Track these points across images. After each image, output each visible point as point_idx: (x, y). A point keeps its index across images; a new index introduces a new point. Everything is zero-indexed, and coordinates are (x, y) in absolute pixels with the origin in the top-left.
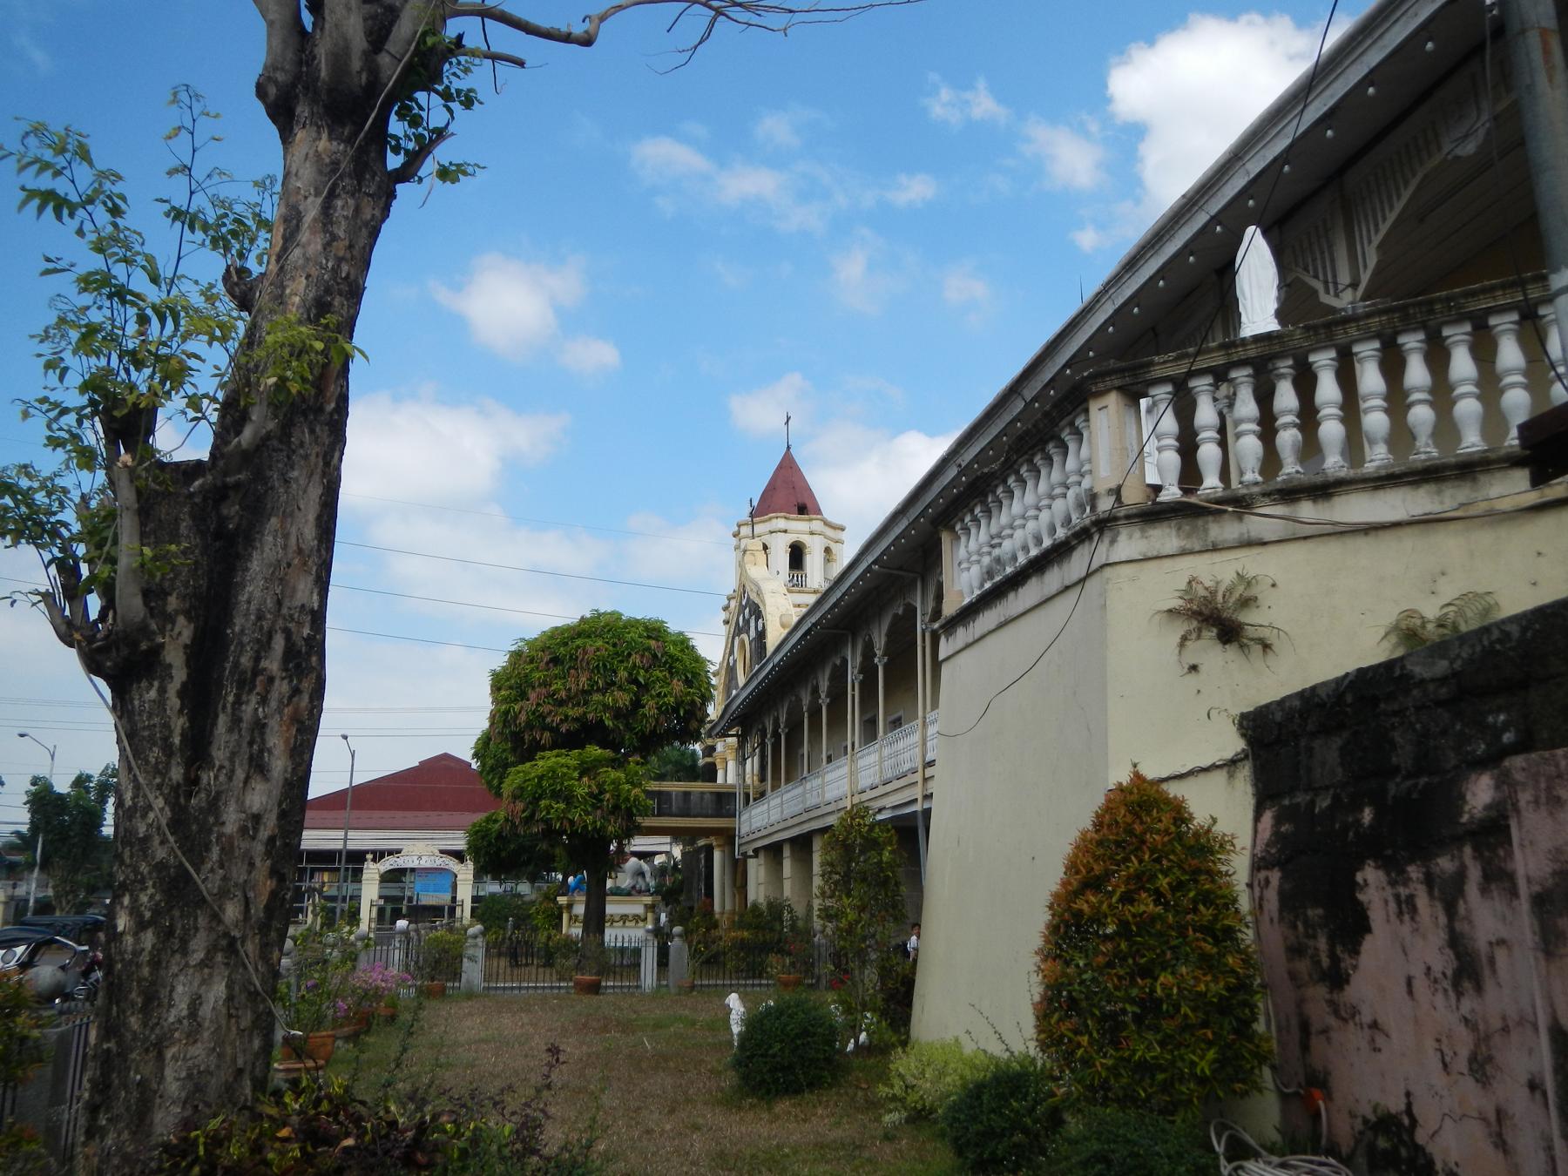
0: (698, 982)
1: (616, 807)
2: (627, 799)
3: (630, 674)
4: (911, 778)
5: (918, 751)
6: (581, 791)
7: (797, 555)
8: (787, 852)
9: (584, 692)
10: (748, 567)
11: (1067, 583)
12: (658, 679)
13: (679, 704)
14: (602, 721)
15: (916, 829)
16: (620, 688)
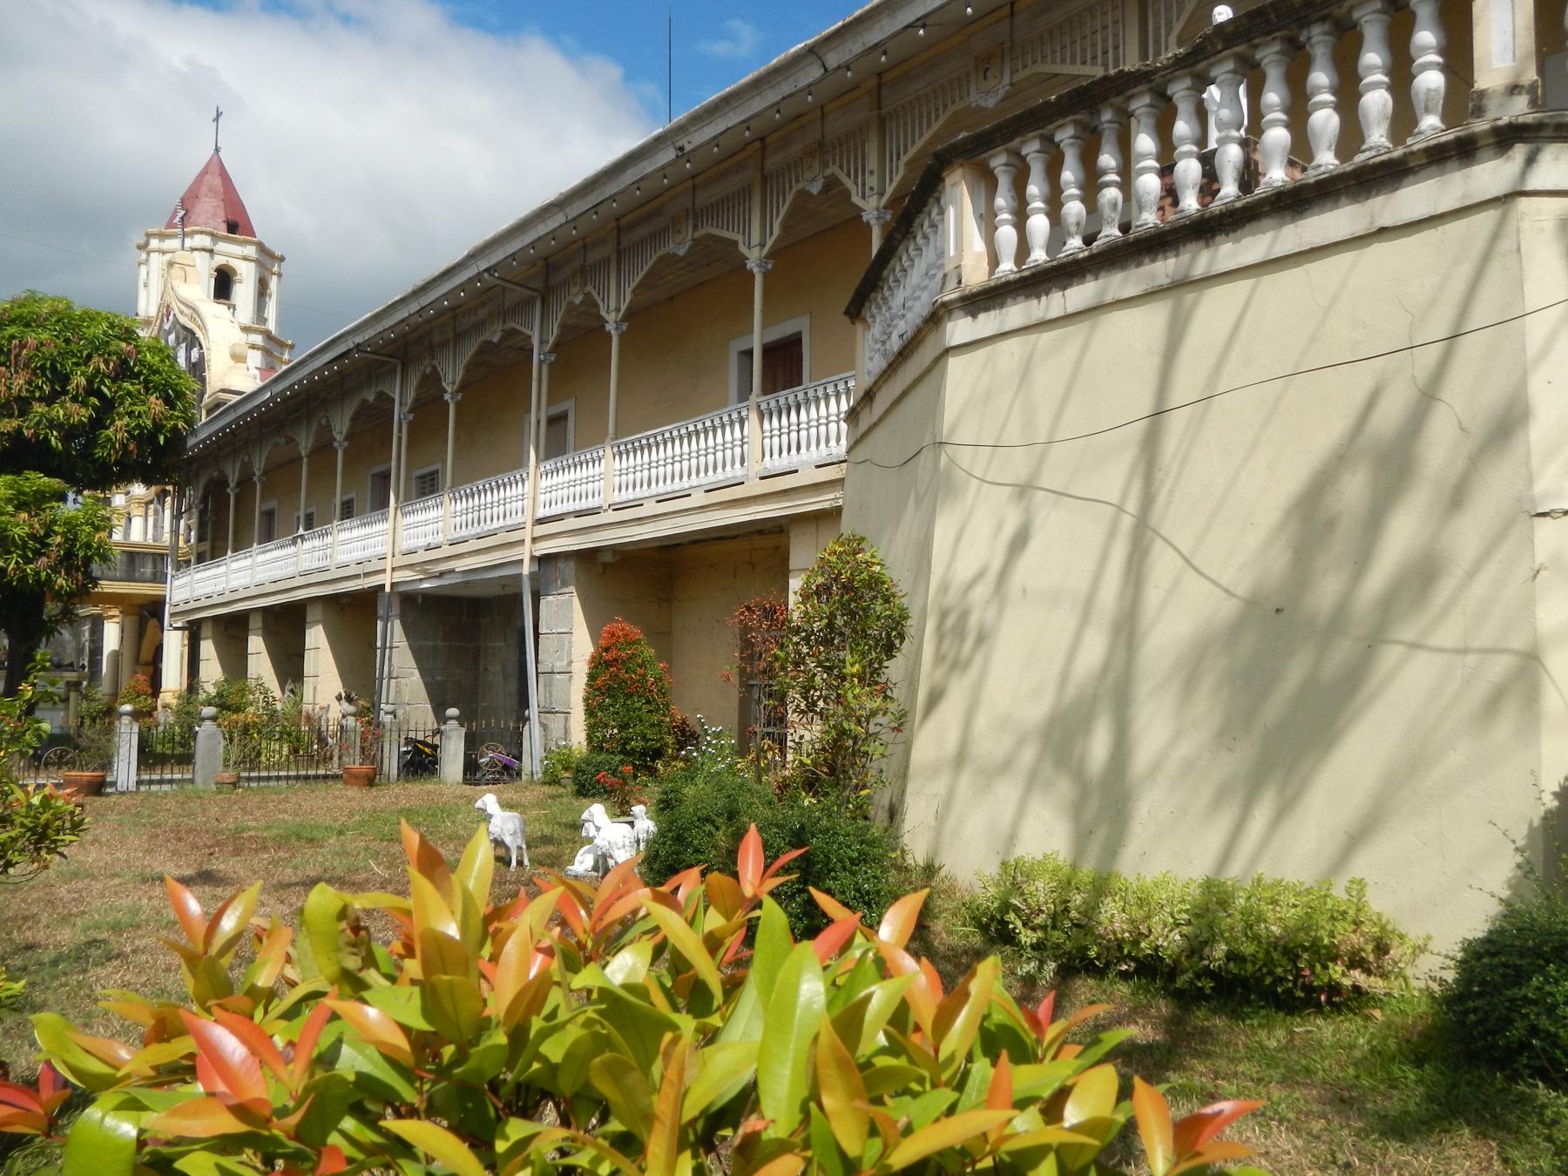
0: (146, 777)
1: (69, 555)
2: (88, 546)
3: (90, 381)
4: (515, 536)
5: (528, 503)
6: (18, 532)
7: (223, 284)
8: (256, 622)
9: (19, 399)
10: (176, 283)
11: (1387, 221)
12: (129, 393)
13: (158, 427)
14: (47, 440)
15: (518, 598)
16: (74, 399)
